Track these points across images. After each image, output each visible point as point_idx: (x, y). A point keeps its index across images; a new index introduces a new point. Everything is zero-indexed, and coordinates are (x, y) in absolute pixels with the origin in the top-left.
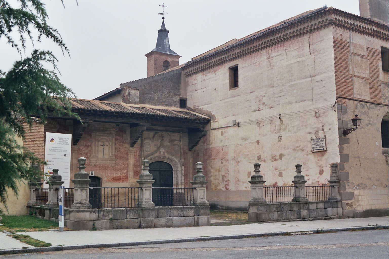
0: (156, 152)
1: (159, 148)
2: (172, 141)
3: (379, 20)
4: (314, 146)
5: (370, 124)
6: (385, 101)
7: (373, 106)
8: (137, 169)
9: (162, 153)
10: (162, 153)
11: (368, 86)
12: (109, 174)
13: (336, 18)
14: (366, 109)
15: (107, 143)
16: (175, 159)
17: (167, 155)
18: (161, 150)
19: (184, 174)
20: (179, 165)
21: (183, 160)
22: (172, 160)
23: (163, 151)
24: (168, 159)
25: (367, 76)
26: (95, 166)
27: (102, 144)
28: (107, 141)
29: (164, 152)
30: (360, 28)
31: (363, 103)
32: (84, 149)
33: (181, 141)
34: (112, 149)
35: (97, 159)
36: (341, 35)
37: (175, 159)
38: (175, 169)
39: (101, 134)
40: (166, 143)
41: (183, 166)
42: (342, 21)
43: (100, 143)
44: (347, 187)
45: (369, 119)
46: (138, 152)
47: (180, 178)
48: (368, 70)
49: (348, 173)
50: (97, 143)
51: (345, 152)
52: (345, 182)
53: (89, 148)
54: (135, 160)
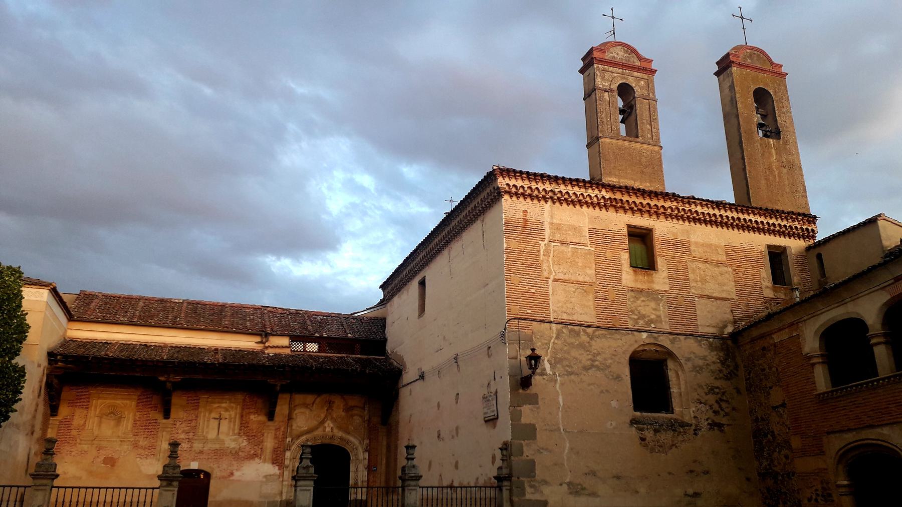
0: (316, 428)
1: (322, 422)
2: (348, 409)
3: (621, 181)
4: (485, 410)
5: (592, 366)
6: (637, 323)
7: (603, 332)
9: (328, 429)
10: (328, 429)
11: (591, 297)
12: (225, 466)
13: (508, 184)
14: (584, 338)
15: (226, 414)
16: (352, 439)
18: (326, 425)
20: (360, 450)
21: (367, 442)
22: (348, 442)
23: (332, 425)
24: (341, 438)
25: (587, 279)
26: (201, 452)
27: (217, 416)
28: (227, 410)
30: (570, 196)
31: (576, 328)
32: (183, 425)
34: (234, 425)
35: (205, 441)
36: (525, 212)
37: (352, 439)
39: (217, 400)
40: (339, 412)
42: (522, 187)
43: (213, 415)
44: (528, 490)
45: (590, 357)
46: (282, 429)
47: (360, 474)
48: (590, 268)
49: (532, 463)
50: (207, 414)
51: (524, 420)
52: (521, 479)
53: (193, 424)
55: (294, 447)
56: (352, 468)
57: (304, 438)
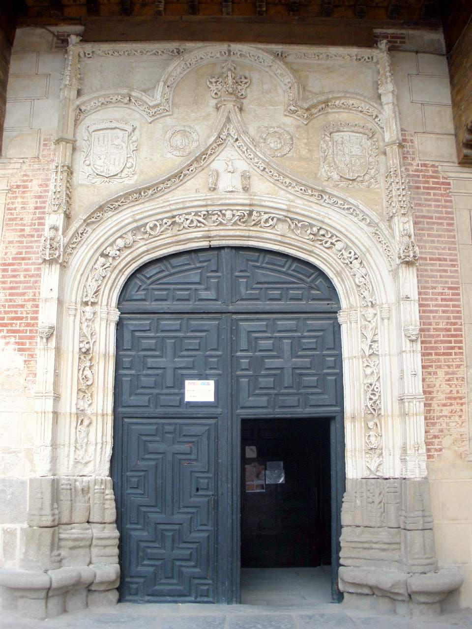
0: (178, 176)
1: (202, 157)
8: (19, 300)
10: (228, 182)
17: (270, 194)
18: (218, 164)
19: (414, 330)
20: (380, 266)
21: (404, 225)
23: (242, 165)
24: (289, 219)
29: (246, 177)
33: (388, 99)
38: (355, 299)
41: (408, 264)
47: (387, 367)
54: (12, 236)
55: (82, 256)
56: (351, 344)
57: (125, 216)
